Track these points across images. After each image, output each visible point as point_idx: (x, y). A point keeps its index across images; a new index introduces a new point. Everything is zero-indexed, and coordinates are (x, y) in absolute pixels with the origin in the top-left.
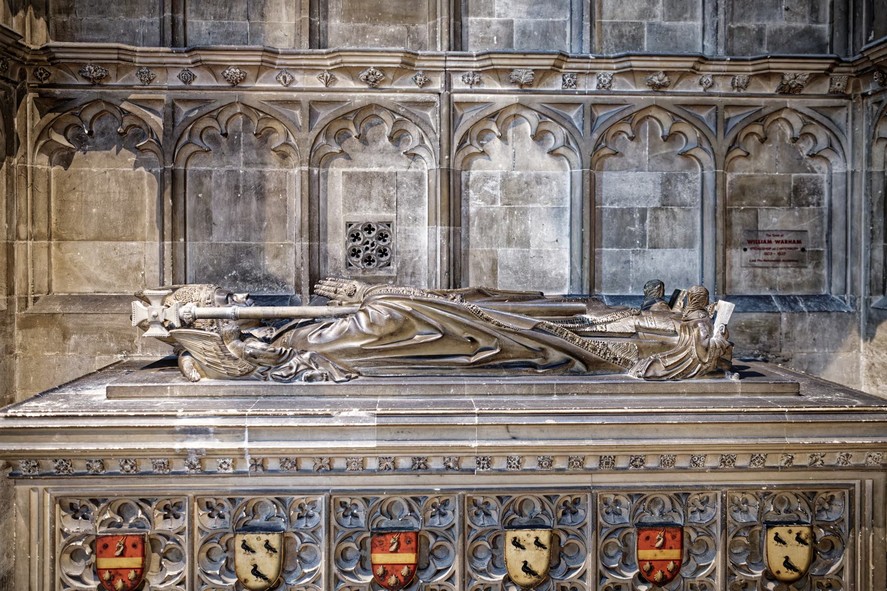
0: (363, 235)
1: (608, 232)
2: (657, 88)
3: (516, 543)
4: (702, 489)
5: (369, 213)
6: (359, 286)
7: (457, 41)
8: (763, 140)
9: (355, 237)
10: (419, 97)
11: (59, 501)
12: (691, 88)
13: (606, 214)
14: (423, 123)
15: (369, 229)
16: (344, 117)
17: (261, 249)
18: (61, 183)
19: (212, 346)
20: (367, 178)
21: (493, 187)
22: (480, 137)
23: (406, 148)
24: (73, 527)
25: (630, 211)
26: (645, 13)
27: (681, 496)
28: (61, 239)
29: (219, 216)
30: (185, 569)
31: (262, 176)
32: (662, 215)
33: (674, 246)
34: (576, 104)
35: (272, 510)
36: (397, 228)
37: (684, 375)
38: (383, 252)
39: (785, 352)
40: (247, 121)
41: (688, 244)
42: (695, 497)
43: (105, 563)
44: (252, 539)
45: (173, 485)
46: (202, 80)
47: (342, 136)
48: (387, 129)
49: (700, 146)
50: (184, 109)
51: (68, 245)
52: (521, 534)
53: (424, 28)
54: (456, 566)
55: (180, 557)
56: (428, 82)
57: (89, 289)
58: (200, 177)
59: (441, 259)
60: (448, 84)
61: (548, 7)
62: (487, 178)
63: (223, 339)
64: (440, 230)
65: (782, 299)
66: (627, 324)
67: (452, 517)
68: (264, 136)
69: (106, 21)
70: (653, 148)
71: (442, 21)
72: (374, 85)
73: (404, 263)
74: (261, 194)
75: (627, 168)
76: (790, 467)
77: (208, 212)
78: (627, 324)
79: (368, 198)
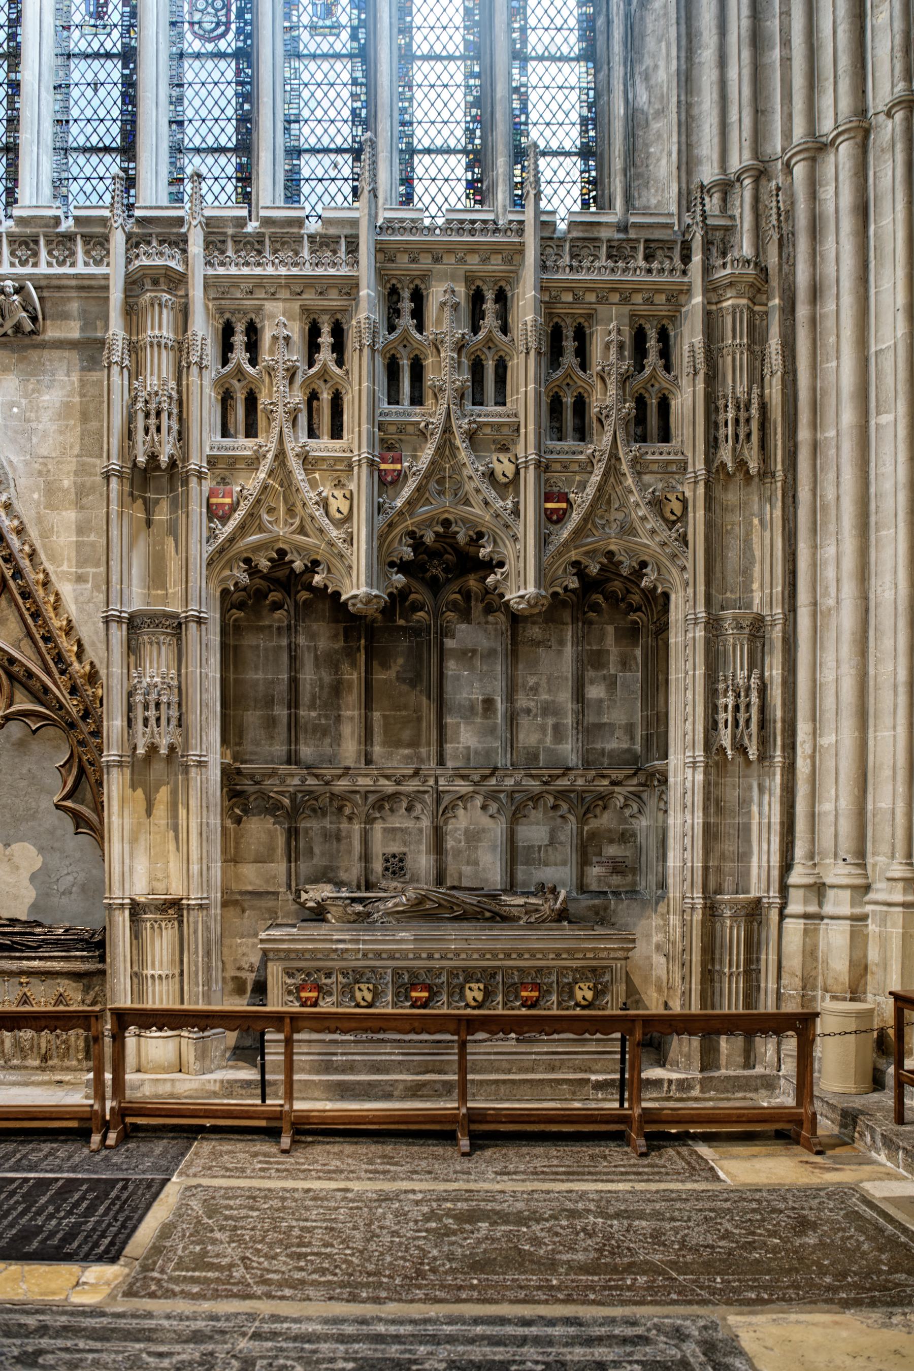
0: (392, 860)
1: (520, 858)
2: (546, 783)
3: (470, 989)
4: (548, 967)
5: (395, 848)
6: (399, 885)
7: (441, 762)
8: (605, 808)
9: (387, 861)
10: (422, 789)
11: (284, 969)
12: (564, 782)
13: (520, 849)
14: (423, 802)
15: (394, 856)
16: (383, 799)
17: (338, 868)
18: (236, 834)
19: (341, 909)
20: (394, 830)
21: (460, 835)
22: (453, 808)
23: (414, 814)
24: (289, 981)
25: (533, 846)
26: (541, 741)
27: (539, 970)
28: (236, 862)
29: (317, 850)
30: (334, 998)
31: (339, 830)
32: (550, 848)
33: (556, 865)
34: (503, 791)
35: (370, 975)
36: (409, 857)
37: (543, 921)
38: (402, 869)
39: (613, 920)
40: (331, 800)
41: (564, 863)
42: (545, 971)
43: (303, 994)
44: (362, 986)
45: (330, 964)
46: (311, 781)
47: (381, 808)
48: (404, 805)
49: (569, 812)
50: (300, 795)
51: (240, 865)
52: (472, 985)
53: (423, 750)
54: (445, 999)
55: (331, 994)
56: (426, 781)
57: (250, 888)
58: (307, 830)
59: (433, 873)
60: (437, 782)
61: (489, 738)
62: (456, 830)
63: (346, 906)
64: (432, 857)
65: (613, 893)
66: (521, 901)
67: (444, 978)
68: (340, 809)
69: (258, 749)
70: (545, 813)
71: (434, 749)
72: (398, 783)
73: (413, 875)
74: (338, 839)
75: (532, 824)
76: (585, 958)
77: (311, 848)
78: (521, 901)
79: (394, 840)
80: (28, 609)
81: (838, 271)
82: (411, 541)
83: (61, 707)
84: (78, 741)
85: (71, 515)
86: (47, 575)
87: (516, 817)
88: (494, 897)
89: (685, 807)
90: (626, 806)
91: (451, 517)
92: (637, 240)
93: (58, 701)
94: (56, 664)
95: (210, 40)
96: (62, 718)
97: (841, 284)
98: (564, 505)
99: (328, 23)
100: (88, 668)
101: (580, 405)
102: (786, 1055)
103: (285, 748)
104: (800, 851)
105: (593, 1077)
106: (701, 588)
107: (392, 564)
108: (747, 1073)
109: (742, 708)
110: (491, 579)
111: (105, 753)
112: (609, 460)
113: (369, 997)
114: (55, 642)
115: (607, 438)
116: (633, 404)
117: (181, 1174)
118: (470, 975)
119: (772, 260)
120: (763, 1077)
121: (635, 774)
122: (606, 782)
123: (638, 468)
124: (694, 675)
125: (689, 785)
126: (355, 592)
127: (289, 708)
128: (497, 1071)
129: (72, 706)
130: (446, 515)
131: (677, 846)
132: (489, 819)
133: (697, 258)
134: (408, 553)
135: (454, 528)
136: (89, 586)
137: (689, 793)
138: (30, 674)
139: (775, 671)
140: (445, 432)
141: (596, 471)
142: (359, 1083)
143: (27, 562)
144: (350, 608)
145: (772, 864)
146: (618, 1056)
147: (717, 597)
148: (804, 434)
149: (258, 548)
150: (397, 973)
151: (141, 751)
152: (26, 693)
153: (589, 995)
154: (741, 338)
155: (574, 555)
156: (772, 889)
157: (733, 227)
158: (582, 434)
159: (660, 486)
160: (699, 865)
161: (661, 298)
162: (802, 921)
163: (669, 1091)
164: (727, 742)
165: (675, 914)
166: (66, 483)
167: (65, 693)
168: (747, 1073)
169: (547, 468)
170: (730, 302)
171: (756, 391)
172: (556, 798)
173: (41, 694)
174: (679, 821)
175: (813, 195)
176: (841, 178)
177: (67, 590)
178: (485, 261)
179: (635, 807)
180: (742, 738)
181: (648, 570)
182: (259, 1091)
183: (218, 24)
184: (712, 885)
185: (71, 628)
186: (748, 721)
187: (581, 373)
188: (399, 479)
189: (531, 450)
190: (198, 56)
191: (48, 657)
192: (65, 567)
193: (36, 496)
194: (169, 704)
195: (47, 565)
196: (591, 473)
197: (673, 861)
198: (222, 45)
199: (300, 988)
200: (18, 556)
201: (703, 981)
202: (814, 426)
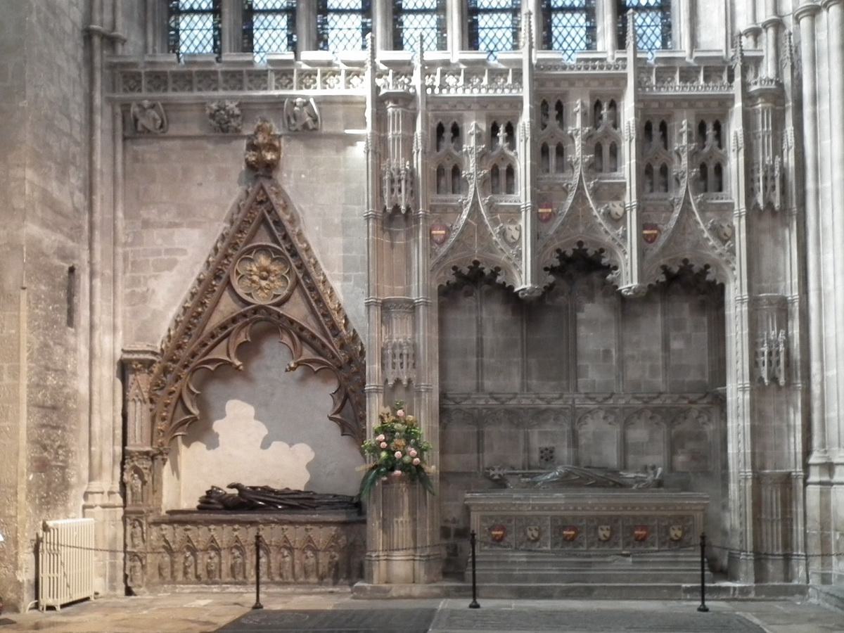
24: (484, 524)
27: (646, 518)
76: (675, 510)
80: (313, 298)
81: (830, 84)
82: (558, 255)
83: (334, 356)
84: (345, 378)
85: (339, 241)
86: (325, 277)
87: (627, 424)
88: (615, 472)
89: (738, 416)
90: (699, 417)
91: (583, 240)
93: (332, 352)
94: (331, 330)
96: (334, 364)
97: (832, 92)
98: (655, 232)
100: (352, 333)
101: (664, 170)
102: (813, 573)
103: (474, 382)
104: (816, 442)
105: (684, 585)
106: (745, 281)
107: (546, 269)
108: (786, 584)
109: (774, 354)
110: (609, 277)
111: (367, 385)
112: (684, 204)
113: (536, 534)
114: (331, 317)
115: (682, 192)
116: (698, 169)
118: (601, 520)
119: (787, 78)
120: (798, 586)
121: (705, 397)
122: (686, 402)
123: (702, 208)
124: (742, 334)
125: (740, 401)
126: (523, 286)
127: (477, 357)
128: (620, 581)
129: (342, 356)
130: (580, 239)
131: (734, 440)
132: (608, 426)
133: (738, 79)
134: (556, 263)
135: (585, 247)
136: (352, 283)
137: (741, 408)
138: (314, 337)
139: (795, 331)
140: (578, 189)
141: (676, 211)
142: (530, 587)
143: (312, 268)
144: (520, 296)
145: (797, 450)
146: (700, 573)
147: (755, 286)
148: (810, 185)
150: (554, 519)
151: (391, 383)
152: (310, 348)
153: (679, 533)
154: (768, 127)
155: (662, 262)
156: (798, 466)
158: (666, 187)
159: (717, 218)
160: (749, 451)
161: (714, 104)
162: (819, 486)
163: (734, 594)
164: (765, 375)
165: (734, 482)
166: (337, 220)
167: (337, 348)
168: (786, 584)
169: (644, 210)
171: (778, 159)
172: (653, 412)
173: (320, 349)
174: (735, 424)
175: (813, 37)
176: (831, 27)
177: (337, 285)
178: (602, 84)
179: (706, 418)
180: (774, 370)
182: (471, 593)
184: (758, 464)
185: (340, 309)
186: (778, 362)
187: (664, 151)
188: (550, 217)
189: (634, 199)
191: (326, 327)
192: (336, 272)
193: (317, 228)
194: (408, 355)
195: (325, 270)
196: (672, 211)
197: (732, 449)
199: (491, 529)
200: (307, 265)
201: (754, 524)
202: (816, 180)
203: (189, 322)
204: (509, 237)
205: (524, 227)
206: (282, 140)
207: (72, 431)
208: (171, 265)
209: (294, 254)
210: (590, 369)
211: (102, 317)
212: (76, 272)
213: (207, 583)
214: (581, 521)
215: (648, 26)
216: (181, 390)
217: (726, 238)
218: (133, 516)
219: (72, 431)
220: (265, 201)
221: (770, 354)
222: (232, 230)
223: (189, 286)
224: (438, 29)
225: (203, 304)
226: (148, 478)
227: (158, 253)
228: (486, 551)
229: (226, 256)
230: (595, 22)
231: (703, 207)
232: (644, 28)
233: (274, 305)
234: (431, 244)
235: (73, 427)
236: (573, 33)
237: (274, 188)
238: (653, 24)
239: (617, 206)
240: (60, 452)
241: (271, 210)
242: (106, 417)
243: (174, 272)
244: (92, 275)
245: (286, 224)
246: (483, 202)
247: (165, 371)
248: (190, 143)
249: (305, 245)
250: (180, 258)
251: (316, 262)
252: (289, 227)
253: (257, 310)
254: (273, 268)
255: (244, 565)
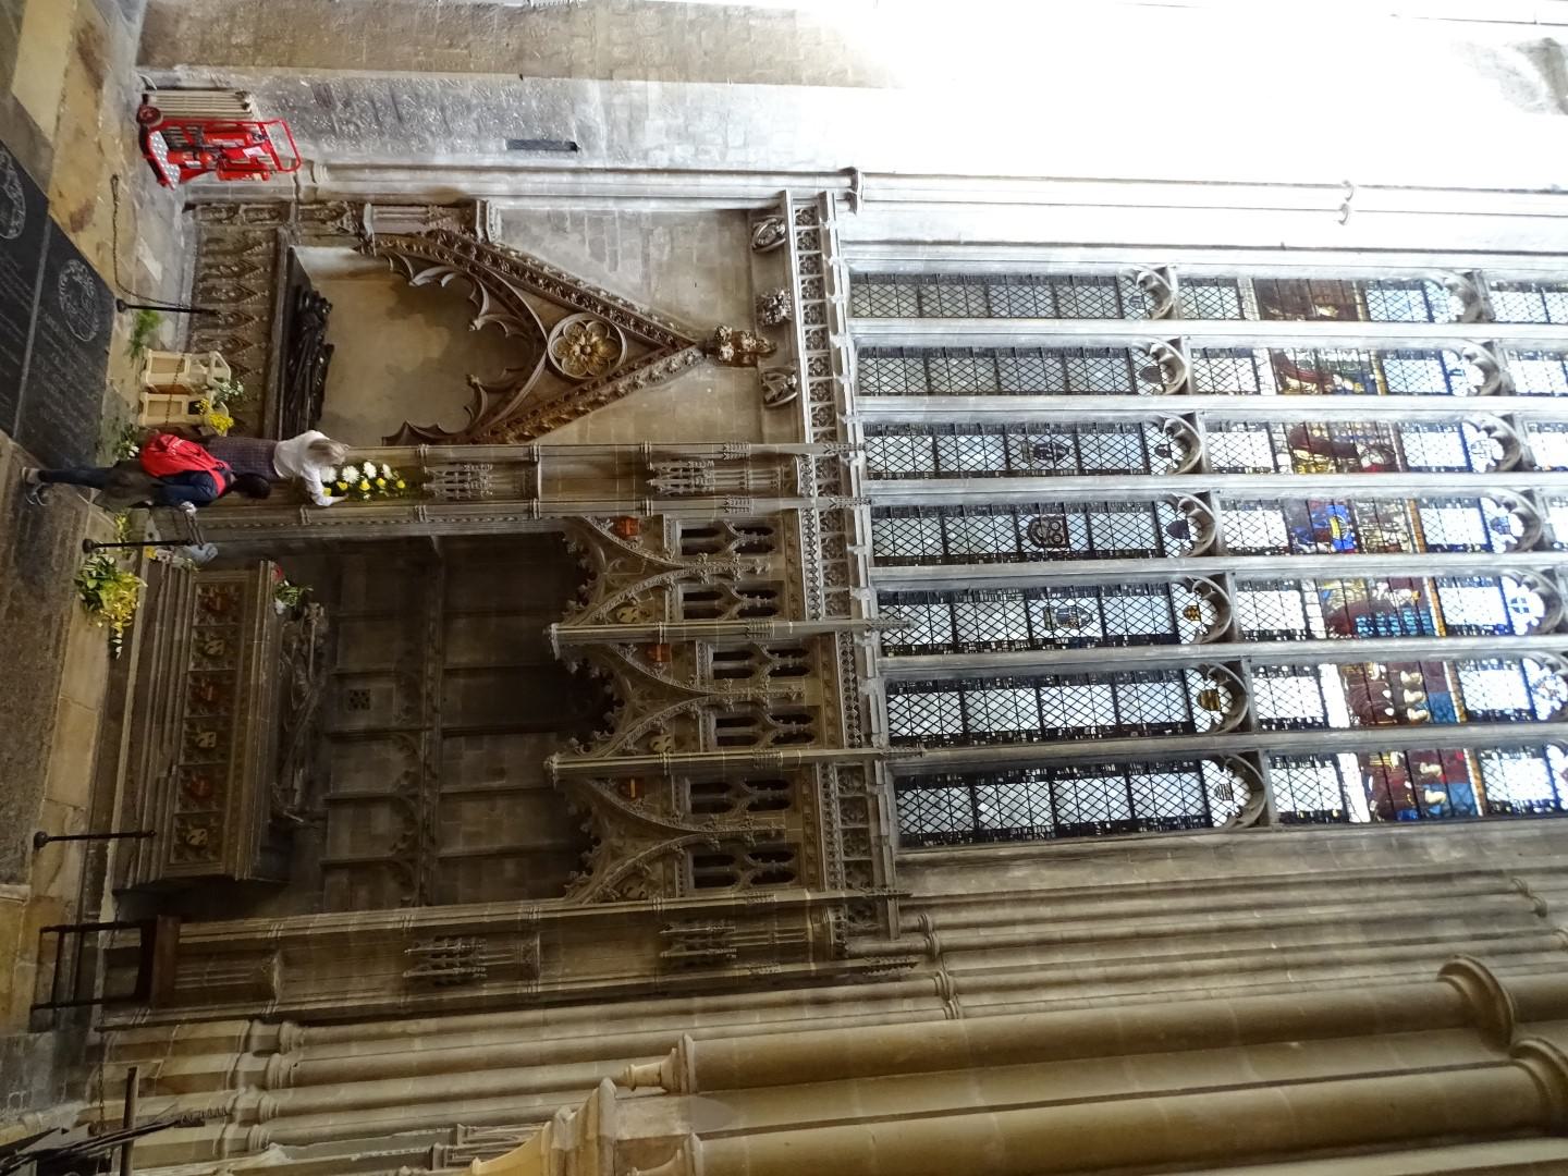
5: (374, 699)
15: (367, 700)
92: (871, 855)
95: (1029, 534)
98: (633, 795)
99: (1054, 621)
107: (586, 661)
117: (16, 451)
135: (616, 708)
148: (698, 1002)
149: (595, 558)
155: (594, 809)
157: (889, 938)
170: (809, 926)
181: (584, 875)
183: (1041, 539)
190: (1016, 525)
195: (591, 415)
198: (1027, 542)
199: (224, 596)
203: (525, 272)
204: (624, 610)
205: (633, 626)
206: (752, 369)
207: (384, 145)
208: (598, 255)
209: (609, 379)
210: (479, 752)
211: (530, 182)
212: (574, 153)
213: (194, 288)
214: (227, 709)
215: (951, 815)
216: (444, 265)
217: (625, 891)
218: (283, 211)
219: (384, 145)
220: (676, 345)
221: (450, 954)
222: (637, 314)
223: (570, 273)
224: (923, 557)
225: (547, 286)
226: (330, 227)
227: (613, 242)
228: (194, 590)
229: (606, 309)
230: (950, 746)
231: (666, 856)
232: (948, 810)
233: (548, 359)
234: (613, 519)
235: (389, 148)
236: (934, 719)
237: (690, 358)
238: (955, 820)
239: (667, 744)
240: (352, 128)
241: (664, 355)
242: (405, 183)
243: (589, 259)
244: (575, 171)
245: (647, 369)
246: (671, 577)
247: (466, 247)
248: (744, 278)
249: (622, 390)
250: (605, 266)
251: (601, 404)
252: (643, 374)
253: (543, 343)
254: (596, 359)
255: (216, 326)
